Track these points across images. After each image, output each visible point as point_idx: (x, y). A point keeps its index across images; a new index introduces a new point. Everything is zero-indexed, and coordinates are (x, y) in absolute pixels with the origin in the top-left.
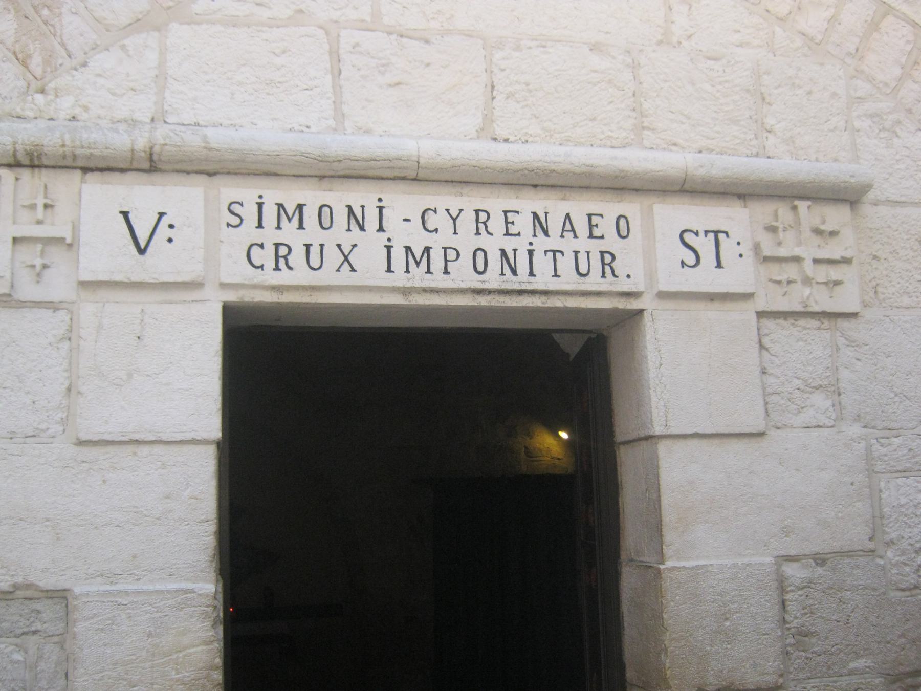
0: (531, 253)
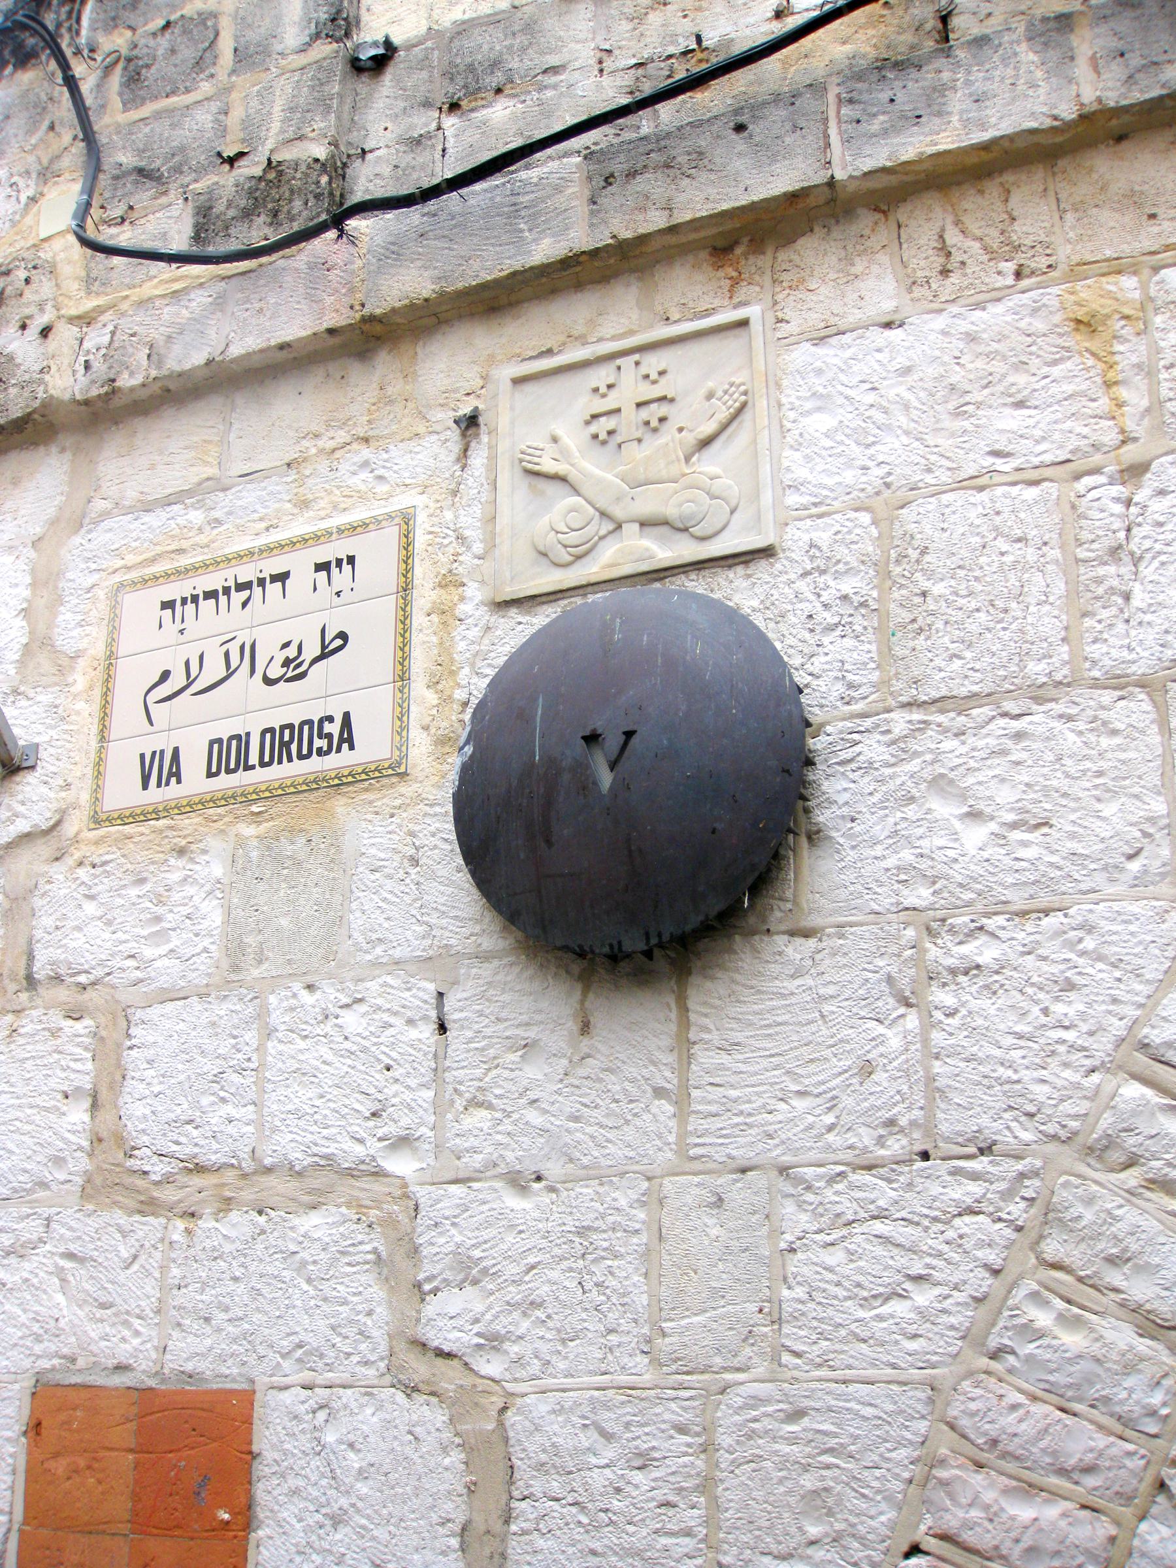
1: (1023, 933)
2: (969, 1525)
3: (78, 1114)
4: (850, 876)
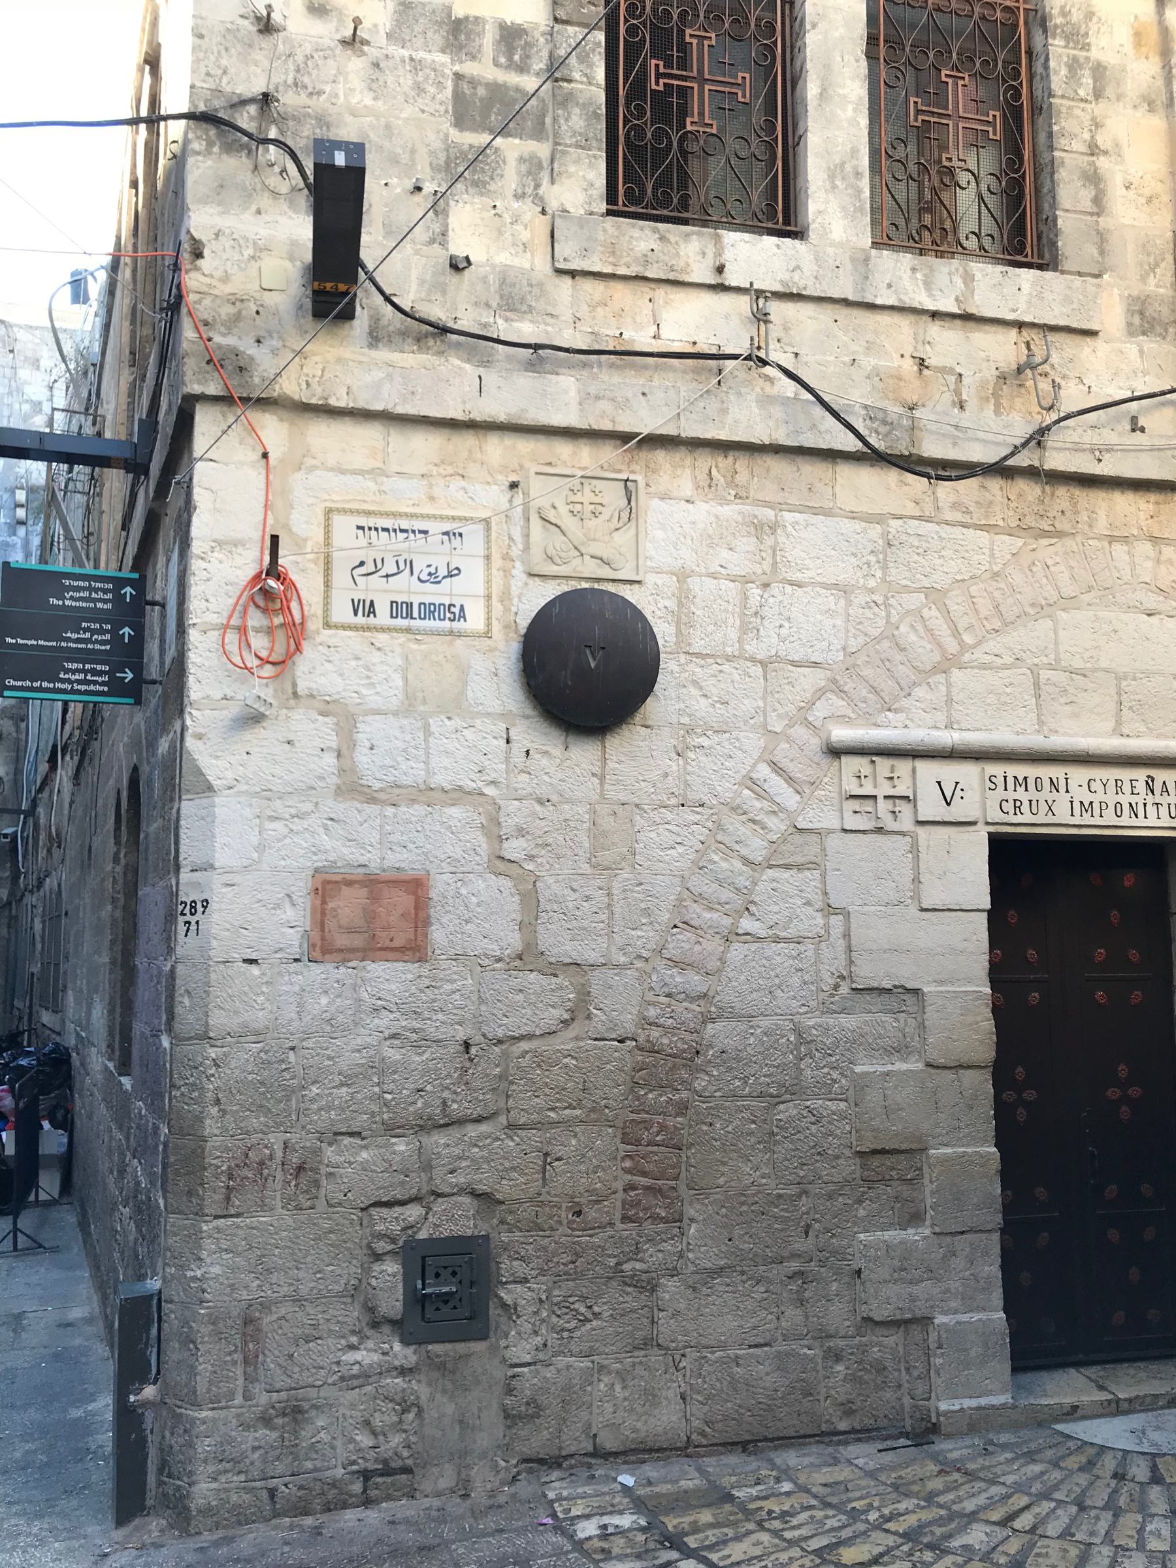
0: (1145, 804)
2: (692, 919)
3: (330, 759)
4: (663, 709)
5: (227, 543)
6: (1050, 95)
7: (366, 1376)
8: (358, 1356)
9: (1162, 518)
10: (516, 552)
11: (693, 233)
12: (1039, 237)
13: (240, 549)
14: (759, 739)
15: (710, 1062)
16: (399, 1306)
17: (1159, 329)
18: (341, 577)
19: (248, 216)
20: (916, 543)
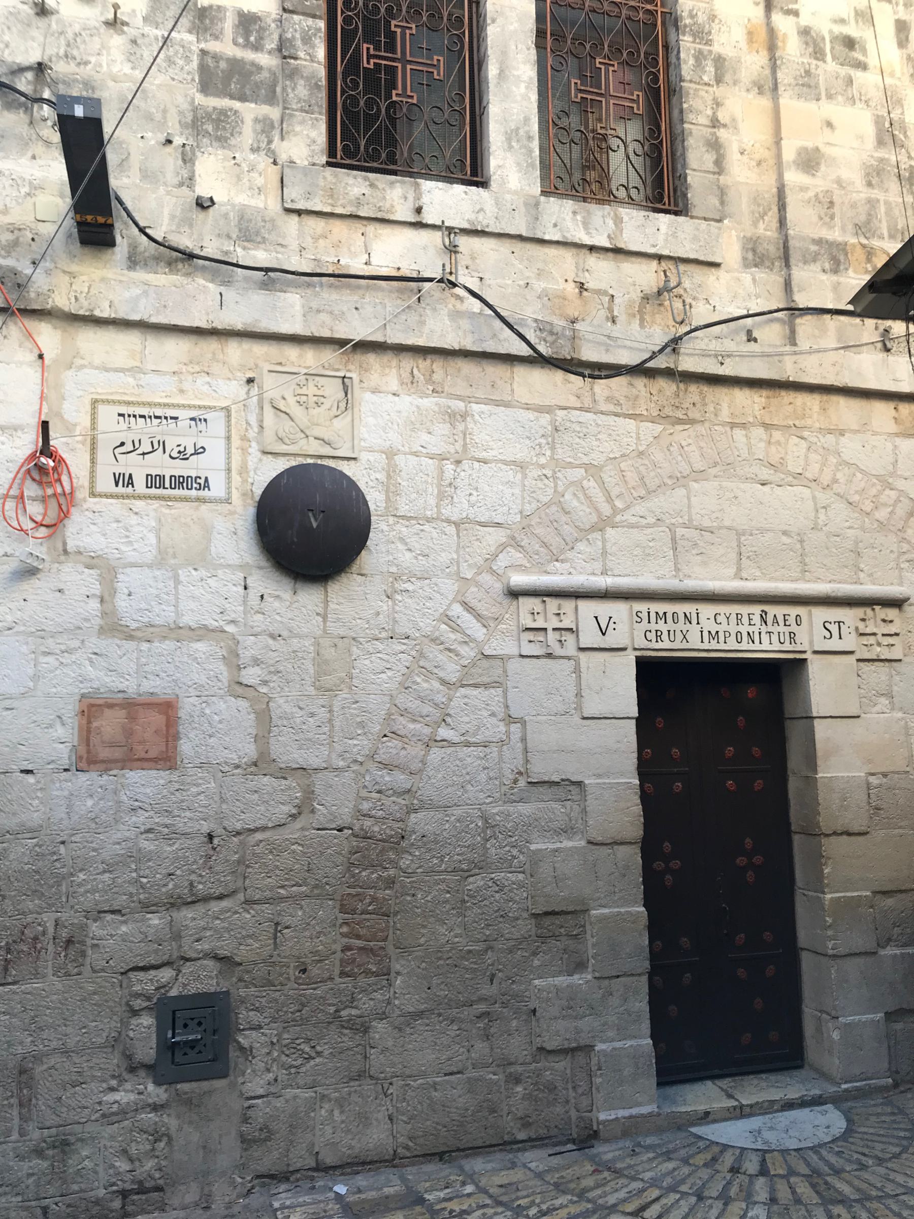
0: (760, 633)
1: (419, 584)
2: (399, 729)
3: (94, 604)
4: (375, 561)
5: (8, 428)
6: (681, 80)
7: (123, 1112)
8: (117, 1096)
9: (772, 409)
10: (252, 434)
11: (398, 181)
12: (675, 190)
13: (19, 433)
14: (454, 584)
15: (413, 844)
16: (153, 1053)
17: (767, 263)
18: (104, 455)
19: (25, 161)
20: (578, 429)
